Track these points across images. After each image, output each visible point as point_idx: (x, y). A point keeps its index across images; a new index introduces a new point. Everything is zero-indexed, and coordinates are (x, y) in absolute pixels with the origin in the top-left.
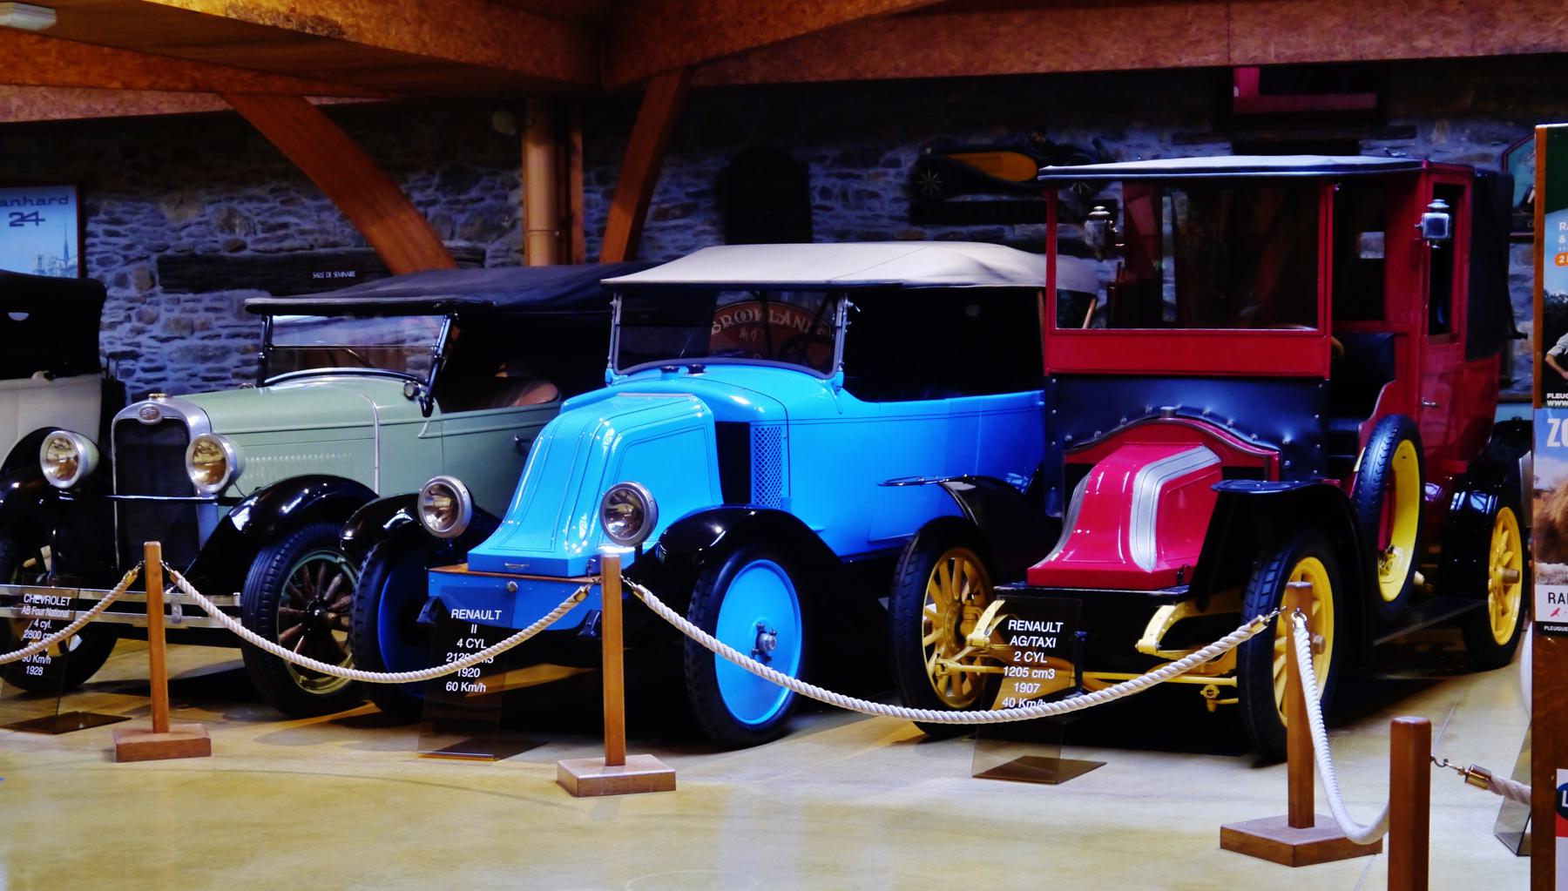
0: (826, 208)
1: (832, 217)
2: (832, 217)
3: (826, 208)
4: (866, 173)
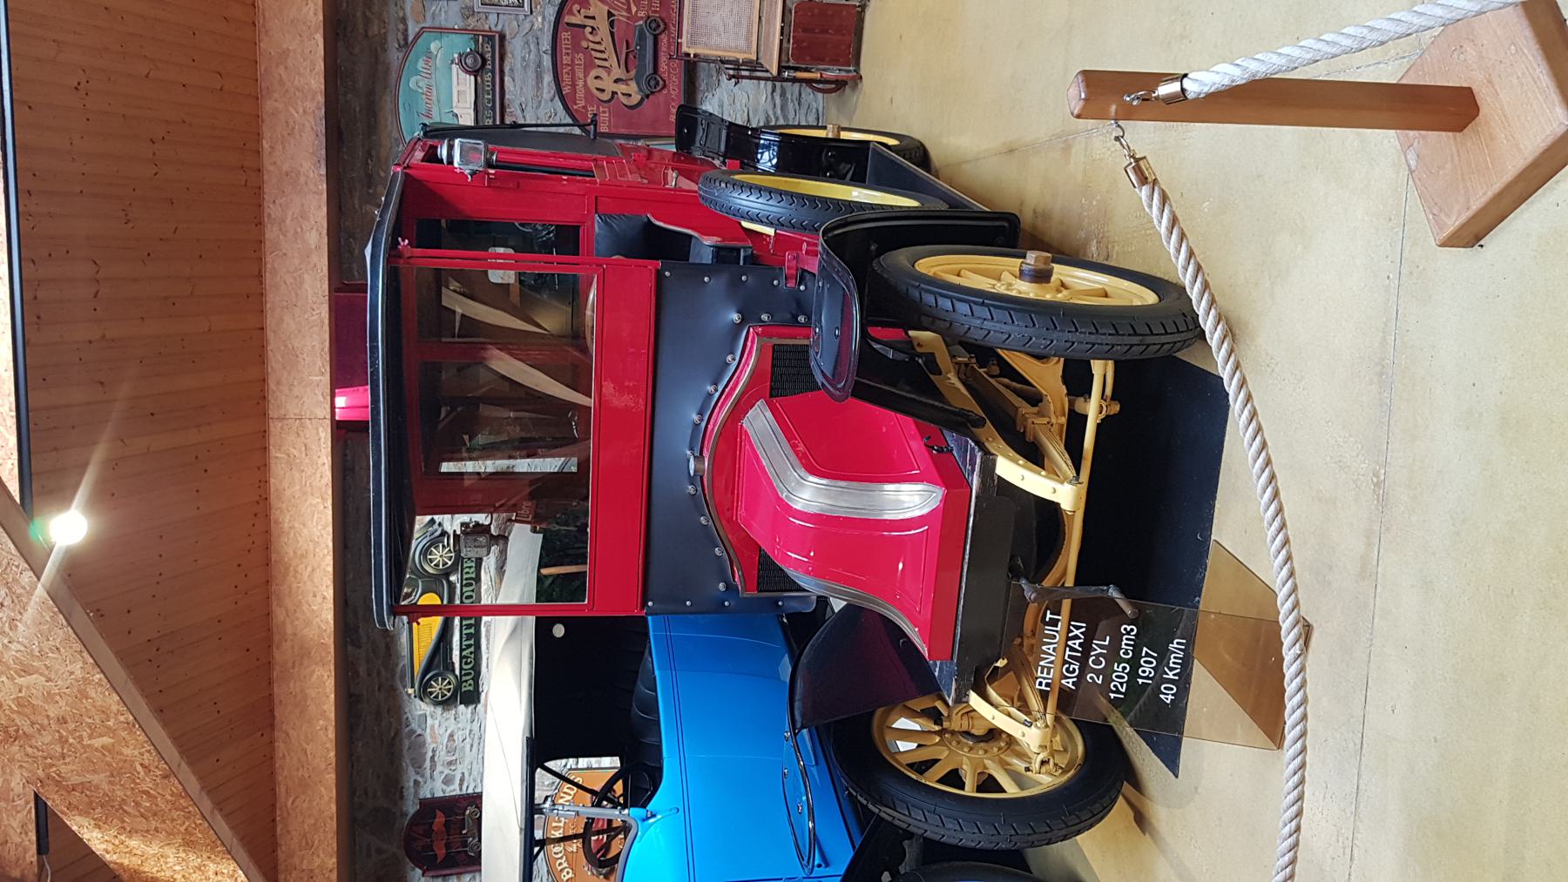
0: (462, 780)
1: (470, 774)
2: (470, 774)
3: (462, 780)
4: (430, 747)
